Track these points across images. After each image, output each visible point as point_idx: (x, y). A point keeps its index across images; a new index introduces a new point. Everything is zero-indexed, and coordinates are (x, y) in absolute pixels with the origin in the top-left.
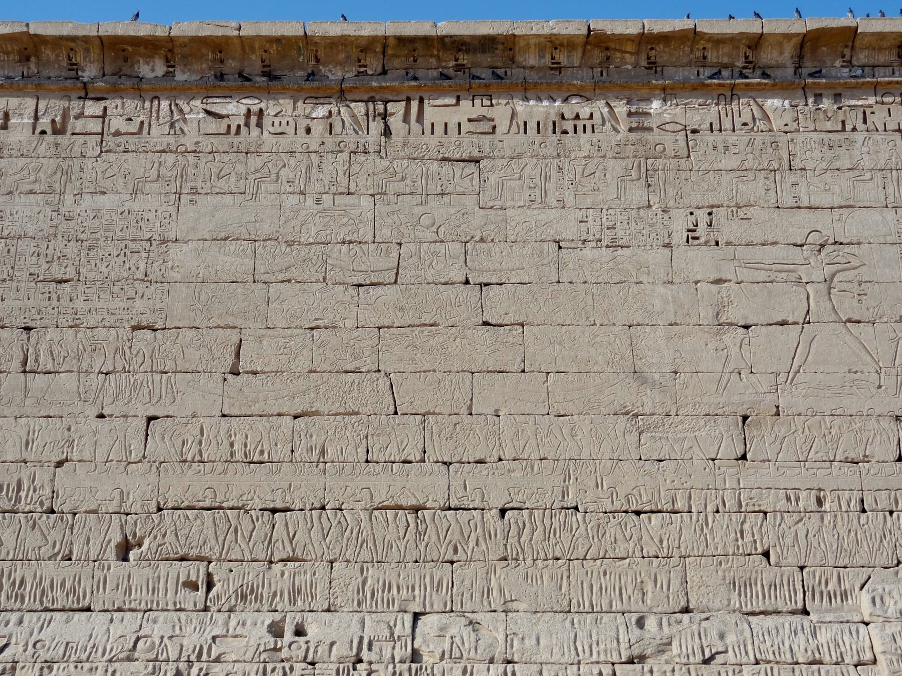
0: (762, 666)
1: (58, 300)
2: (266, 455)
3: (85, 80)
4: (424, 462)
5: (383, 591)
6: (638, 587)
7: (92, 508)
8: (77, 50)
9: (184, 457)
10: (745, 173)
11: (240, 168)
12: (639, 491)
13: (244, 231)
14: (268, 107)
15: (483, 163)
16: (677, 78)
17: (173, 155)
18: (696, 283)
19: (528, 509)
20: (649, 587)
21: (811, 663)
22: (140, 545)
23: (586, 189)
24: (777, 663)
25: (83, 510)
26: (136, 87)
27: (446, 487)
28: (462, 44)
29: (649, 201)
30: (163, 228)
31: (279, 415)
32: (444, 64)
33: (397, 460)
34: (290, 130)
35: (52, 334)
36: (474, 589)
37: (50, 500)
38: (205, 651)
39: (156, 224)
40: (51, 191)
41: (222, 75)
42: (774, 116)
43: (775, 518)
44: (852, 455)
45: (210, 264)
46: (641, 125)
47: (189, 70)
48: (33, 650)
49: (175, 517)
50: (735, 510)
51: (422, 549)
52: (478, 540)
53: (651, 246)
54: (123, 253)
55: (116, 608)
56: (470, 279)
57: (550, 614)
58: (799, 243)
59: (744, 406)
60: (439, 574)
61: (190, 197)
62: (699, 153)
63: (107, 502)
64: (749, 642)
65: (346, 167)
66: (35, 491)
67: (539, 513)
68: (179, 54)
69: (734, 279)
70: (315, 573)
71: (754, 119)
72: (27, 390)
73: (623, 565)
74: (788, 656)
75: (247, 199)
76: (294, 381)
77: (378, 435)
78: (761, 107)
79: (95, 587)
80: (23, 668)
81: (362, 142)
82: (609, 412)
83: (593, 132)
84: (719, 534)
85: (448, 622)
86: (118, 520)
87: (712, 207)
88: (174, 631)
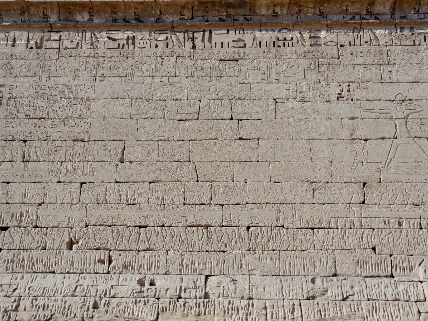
0: (371, 302)
1: (39, 128)
2: (136, 201)
3: (51, 22)
4: (211, 204)
5: (191, 265)
6: (312, 264)
7: (55, 225)
8: (47, 8)
9: (98, 202)
10: (366, 66)
11: (124, 64)
12: (313, 218)
13: (126, 94)
14: (137, 35)
15: (240, 62)
16: (334, 20)
17: (93, 59)
18: (342, 119)
19: (260, 226)
20: (318, 264)
21: (394, 301)
22: (78, 243)
23: (289, 74)
24: (378, 300)
25: (51, 226)
26: (75, 26)
28: (230, 4)
29: (319, 79)
30: (88, 93)
31: (143, 182)
32: (221, 14)
33: (198, 203)
34: (148, 46)
35: (36, 144)
36: (234, 264)
37: (36, 221)
38: (108, 292)
40: (35, 75)
41: (115, 20)
42: (381, 38)
43: (378, 232)
44: (416, 202)
46: (316, 43)
47: (100, 18)
48: (28, 291)
49: (94, 229)
50: (359, 228)
51: (210, 245)
52: (236, 241)
53: (320, 101)
54: (69, 105)
55: (66, 272)
57: (270, 276)
58: (392, 100)
59: (364, 178)
60: (218, 257)
61: (101, 78)
62: (344, 56)
63: (62, 222)
64: (365, 290)
65: (174, 64)
66: (29, 217)
67: (265, 229)
68: (95, 10)
69: (360, 117)
70: (159, 256)
71: (371, 39)
72: (25, 170)
73: (305, 253)
74: (384, 297)
75: (128, 79)
76: (149, 166)
77: (190, 191)
78: (374, 34)
79: (57, 262)
80: (24, 299)
81: (182, 51)
82: (299, 181)
83: (293, 46)
84: (351, 239)
85: (222, 280)
86: (67, 231)
87: (350, 82)
88: (93, 283)
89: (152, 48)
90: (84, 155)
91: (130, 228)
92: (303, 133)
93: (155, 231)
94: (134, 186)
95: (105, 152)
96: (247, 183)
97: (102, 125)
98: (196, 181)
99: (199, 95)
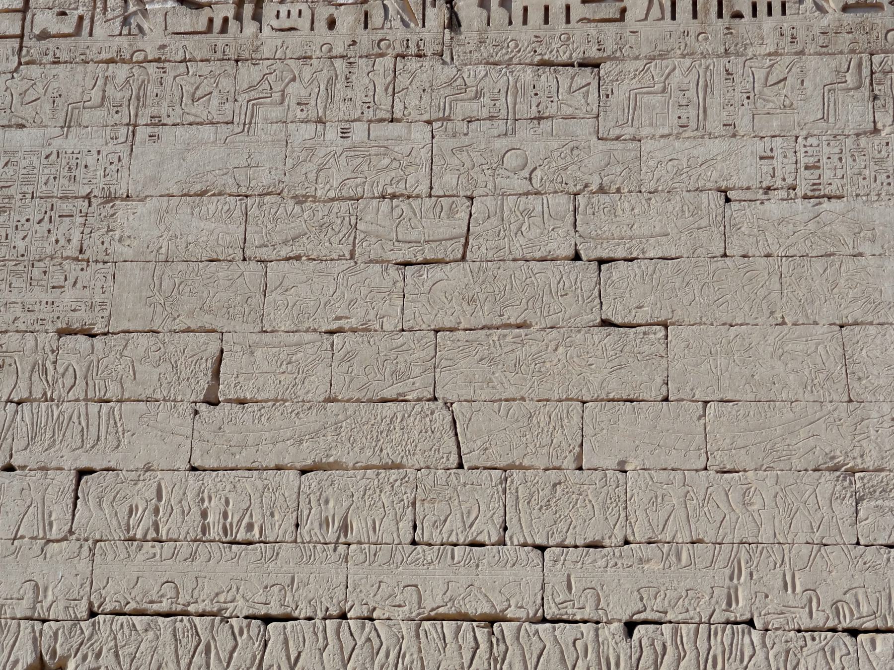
4: (505, 545)
9: (132, 533)
11: (226, 84)
12: (856, 595)
13: (231, 181)
15: (604, 68)
17: (126, 67)
19: (670, 622)
23: (771, 105)
27: (539, 586)
29: (874, 122)
30: (108, 178)
31: (278, 468)
33: (461, 541)
34: (304, 23)
39: (98, 173)
45: (178, 233)
53: (879, 195)
56: (582, 252)
61: (150, 130)
63: (15, 601)
65: (389, 79)
67: (689, 630)
75: (237, 130)
76: (301, 415)
77: (433, 501)
82: (805, 466)
83: (784, 13)
86: (29, 630)
89: (316, 31)
90: (89, 379)
91: (233, 621)
92: (818, 303)
93: (316, 634)
94: (250, 483)
95: (158, 370)
96: (626, 472)
97: (151, 280)
98: (455, 465)
99: (470, 179)
